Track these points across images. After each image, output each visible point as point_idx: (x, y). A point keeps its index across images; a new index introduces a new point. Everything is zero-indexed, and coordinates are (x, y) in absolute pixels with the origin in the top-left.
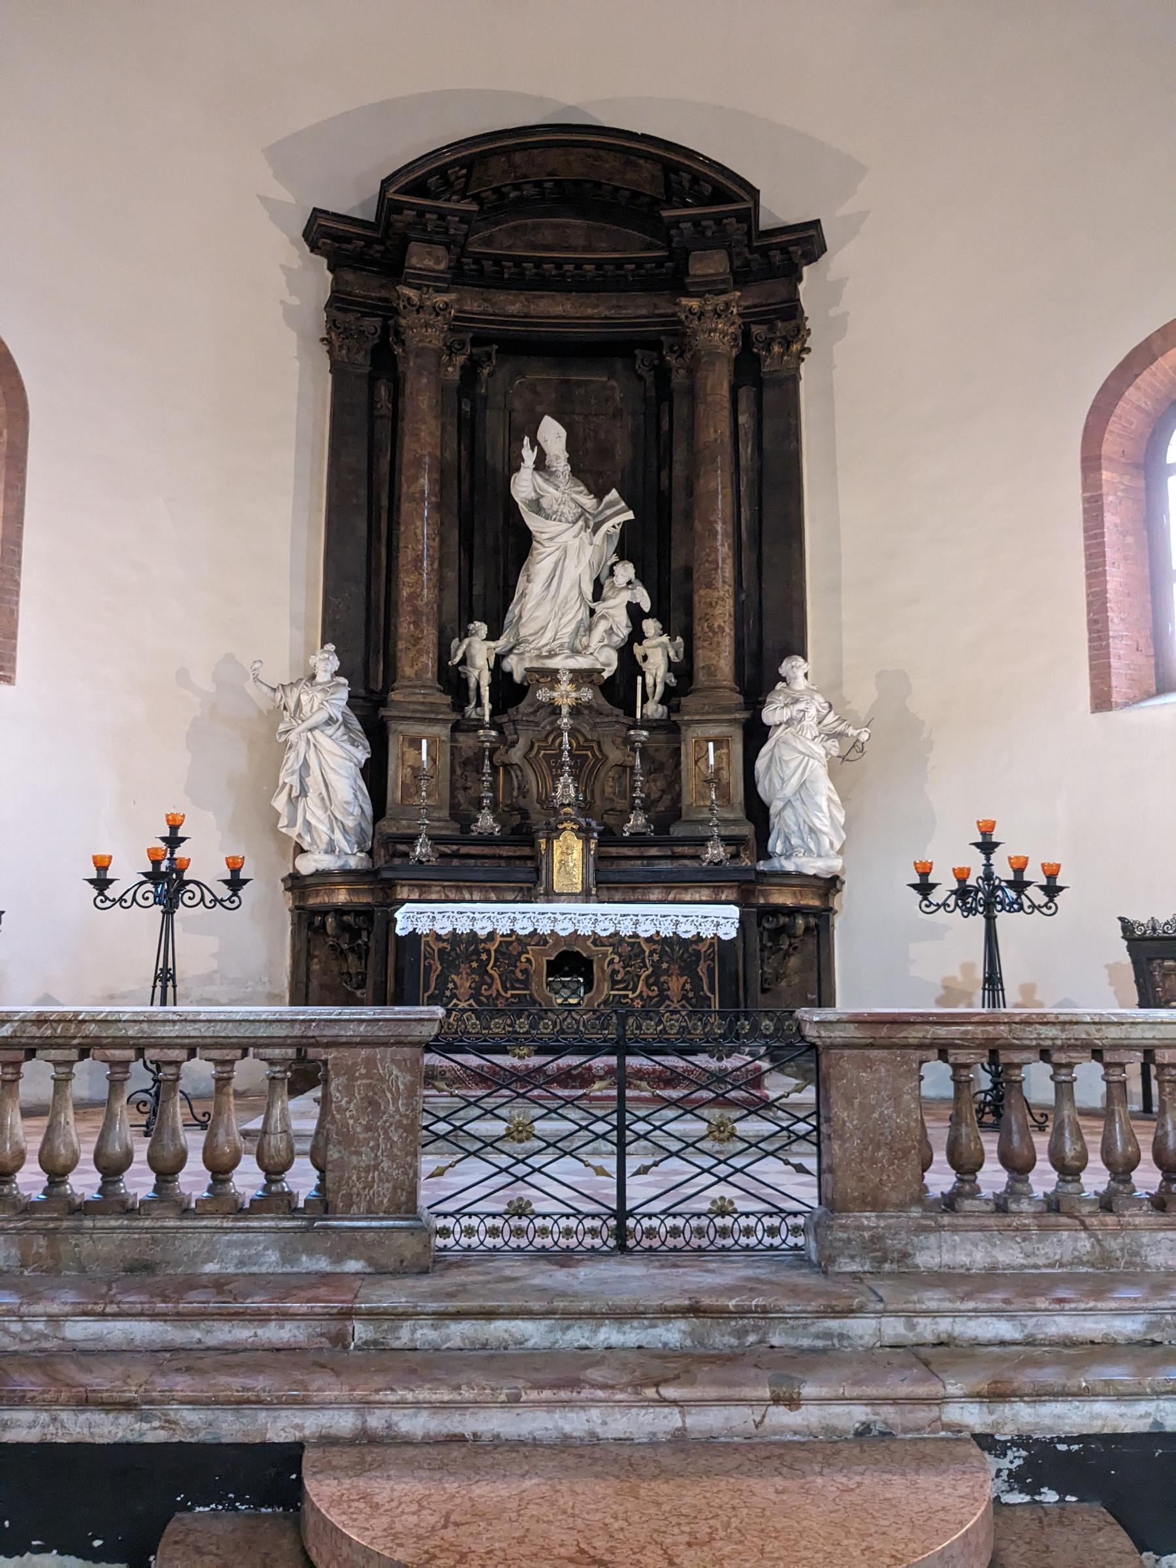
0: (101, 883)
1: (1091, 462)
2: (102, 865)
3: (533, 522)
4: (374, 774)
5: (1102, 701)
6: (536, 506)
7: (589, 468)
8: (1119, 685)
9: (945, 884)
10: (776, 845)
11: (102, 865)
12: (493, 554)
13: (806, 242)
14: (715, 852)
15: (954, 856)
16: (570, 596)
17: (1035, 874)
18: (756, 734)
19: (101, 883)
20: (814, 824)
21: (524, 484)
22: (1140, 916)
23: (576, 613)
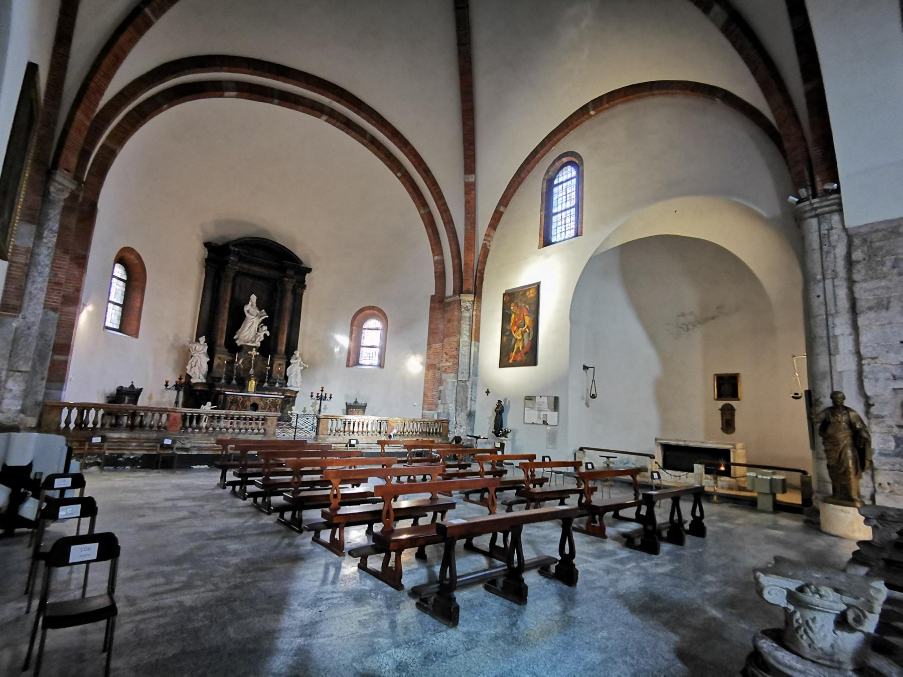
0: (166, 385)
1: (352, 325)
2: (167, 382)
3: (247, 314)
4: (210, 364)
5: (348, 366)
6: (248, 311)
7: (259, 306)
8: (351, 363)
9: (315, 395)
10: (288, 384)
11: (167, 382)
12: (238, 319)
13: (309, 270)
14: (277, 385)
15: (317, 391)
16: (252, 331)
17: (328, 396)
18: (288, 364)
19: (166, 385)
20: (295, 381)
21: (246, 308)
22: (348, 402)
23: (253, 334)
